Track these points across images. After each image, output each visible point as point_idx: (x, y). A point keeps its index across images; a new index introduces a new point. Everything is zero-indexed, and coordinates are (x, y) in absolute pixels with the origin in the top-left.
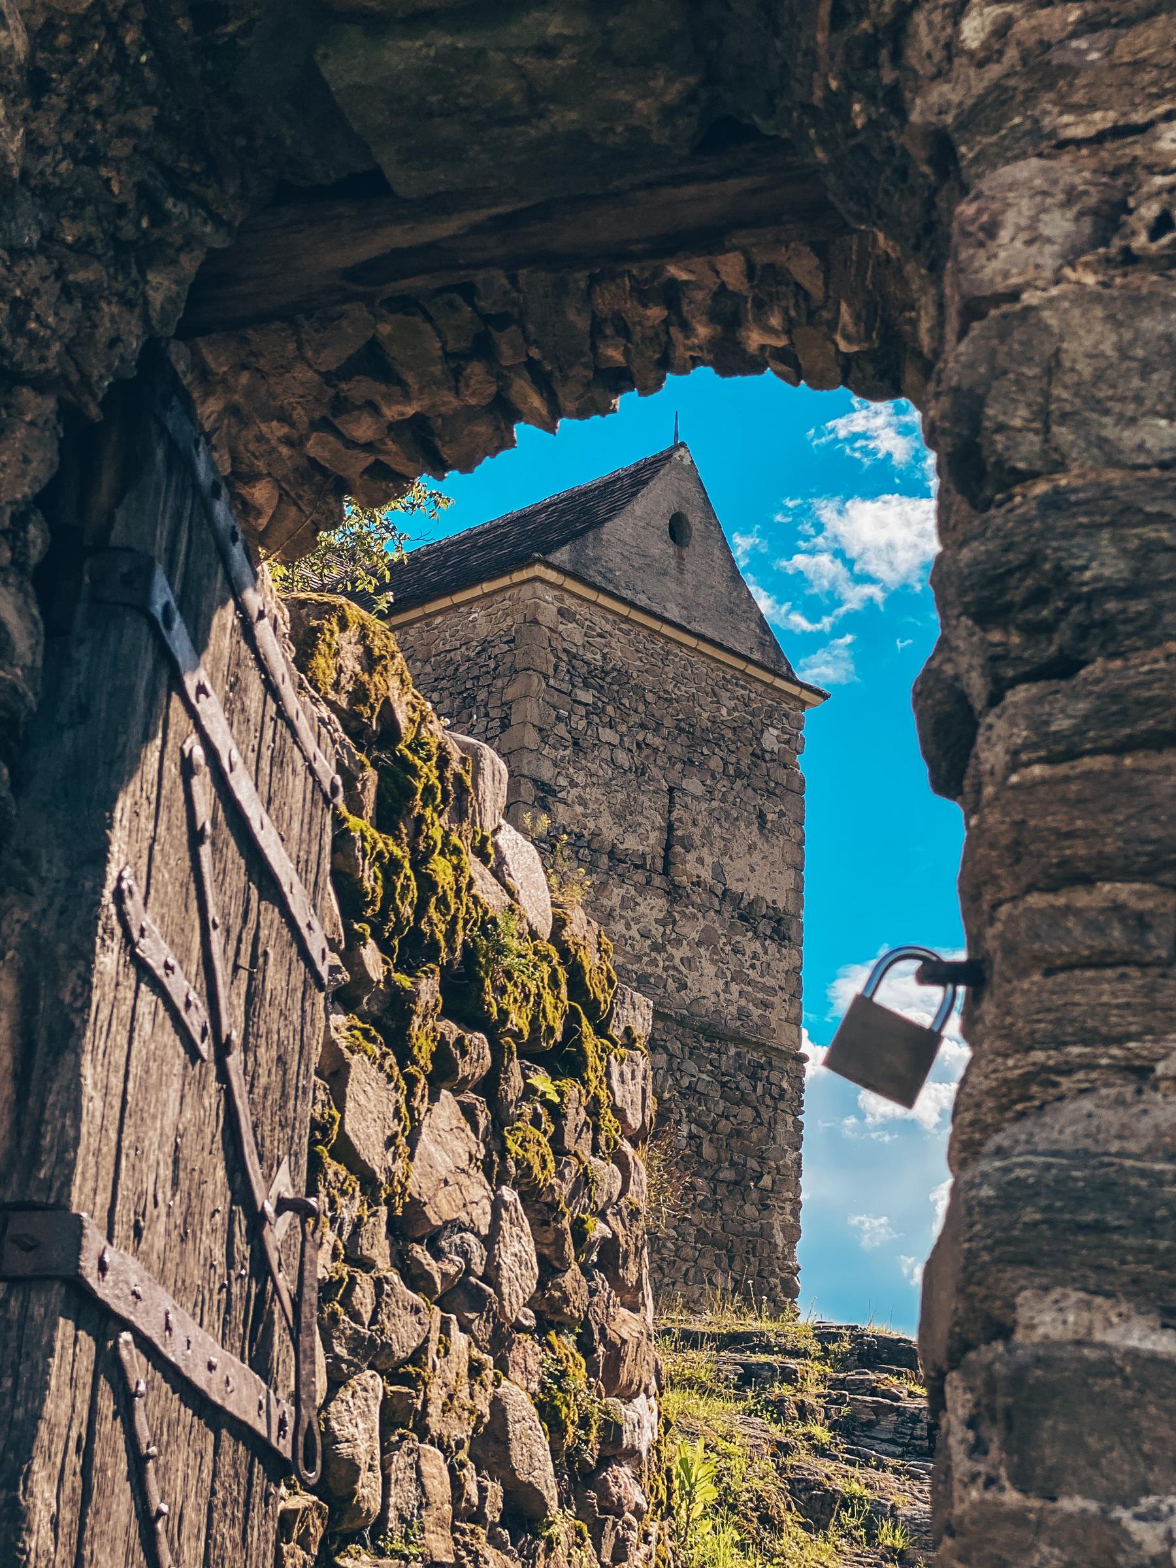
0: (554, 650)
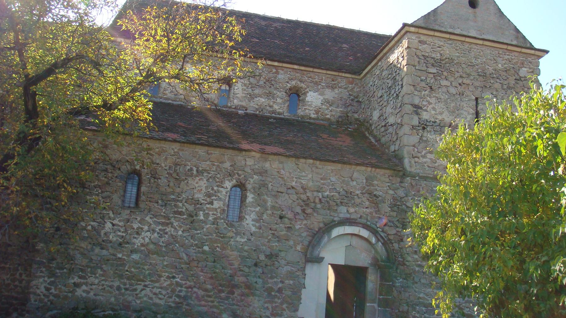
0: (417, 56)
